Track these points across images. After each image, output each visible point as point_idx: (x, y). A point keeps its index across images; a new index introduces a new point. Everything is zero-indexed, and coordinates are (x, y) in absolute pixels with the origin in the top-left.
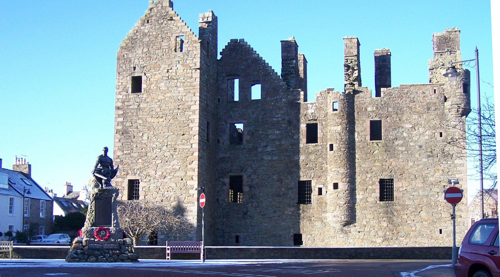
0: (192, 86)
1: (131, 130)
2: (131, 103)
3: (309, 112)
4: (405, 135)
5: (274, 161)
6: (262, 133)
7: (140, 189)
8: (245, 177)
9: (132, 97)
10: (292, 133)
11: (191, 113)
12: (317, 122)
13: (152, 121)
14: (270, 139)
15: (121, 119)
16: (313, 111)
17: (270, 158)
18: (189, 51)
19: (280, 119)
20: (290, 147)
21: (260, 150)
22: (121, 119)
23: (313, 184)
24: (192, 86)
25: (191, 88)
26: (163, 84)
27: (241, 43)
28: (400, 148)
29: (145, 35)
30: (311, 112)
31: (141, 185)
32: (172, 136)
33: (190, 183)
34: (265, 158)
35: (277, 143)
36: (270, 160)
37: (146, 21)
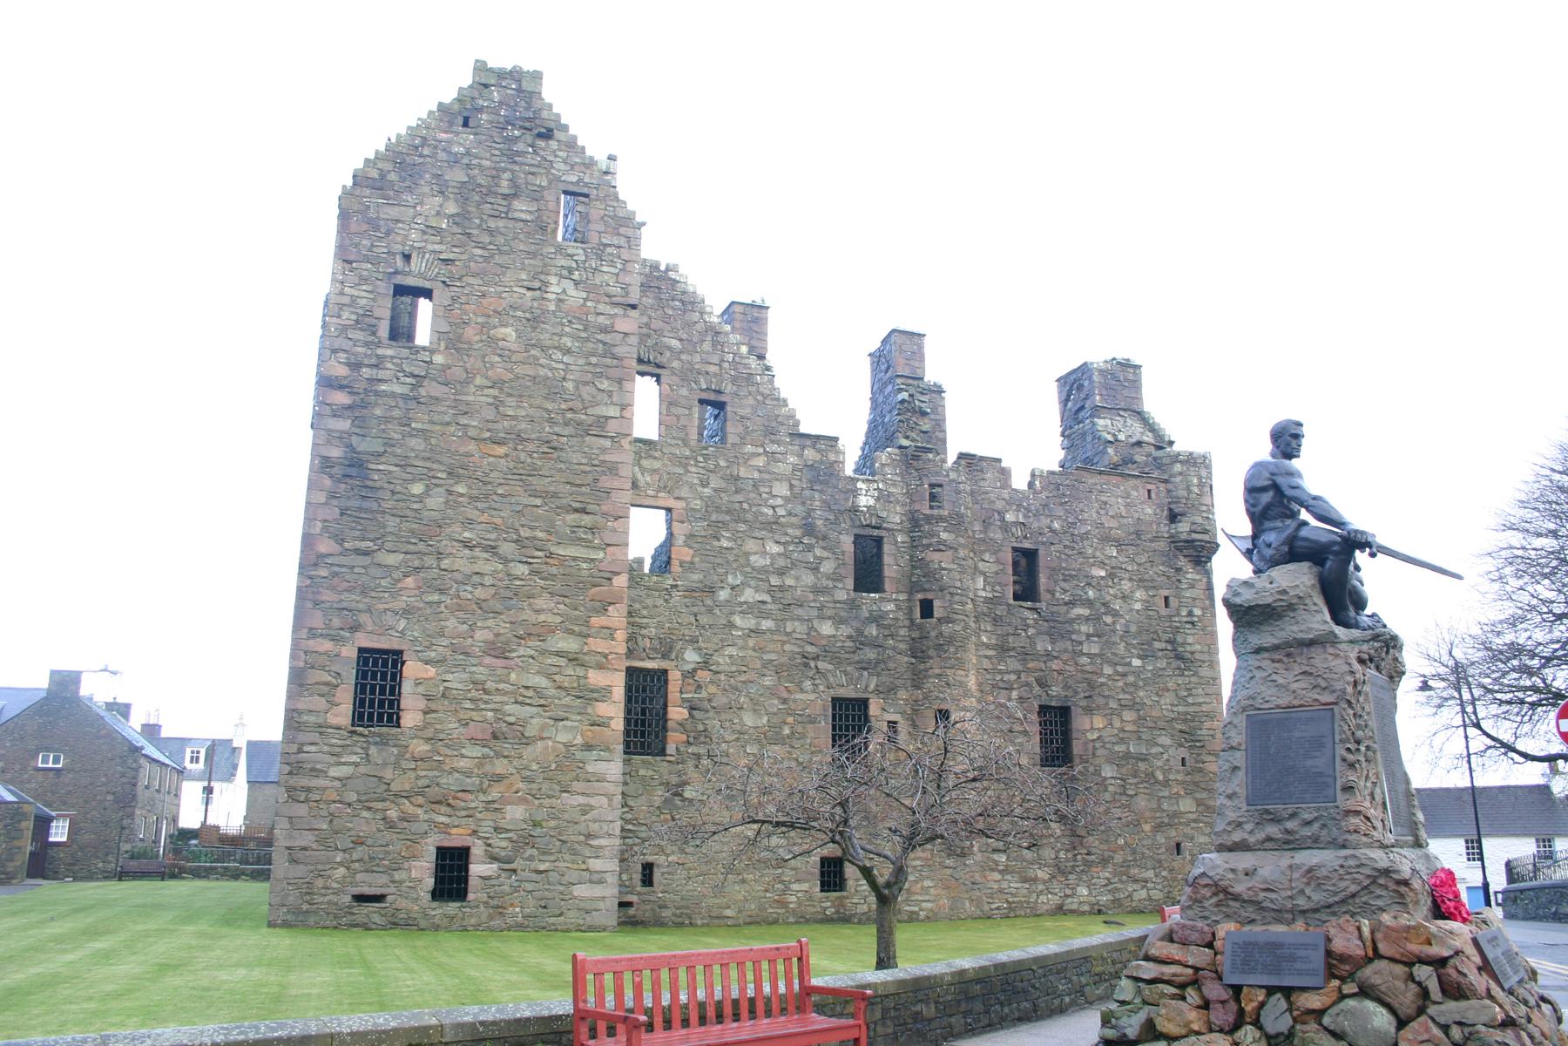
0: (614, 357)
1: (381, 467)
2: (381, 374)
3: (862, 504)
4: (1091, 593)
5: (764, 632)
6: (730, 545)
7: (407, 687)
8: (675, 677)
9: (389, 352)
10: (815, 557)
11: (608, 443)
12: (883, 533)
13: (462, 450)
14: (753, 569)
15: (344, 425)
16: (872, 502)
17: (751, 622)
18: (606, 245)
19: (781, 512)
20: (811, 596)
21: (723, 595)
22: (344, 425)
23: (874, 710)
24: (614, 357)
25: (608, 361)
26: (509, 332)
27: (672, 275)
28: (1084, 628)
29: (455, 160)
30: (865, 504)
31: (412, 669)
32: (535, 509)
33: (595, 678)
34: (737, 620)
35: (774, 581)
36: (751, 630)
37: (460, 121)
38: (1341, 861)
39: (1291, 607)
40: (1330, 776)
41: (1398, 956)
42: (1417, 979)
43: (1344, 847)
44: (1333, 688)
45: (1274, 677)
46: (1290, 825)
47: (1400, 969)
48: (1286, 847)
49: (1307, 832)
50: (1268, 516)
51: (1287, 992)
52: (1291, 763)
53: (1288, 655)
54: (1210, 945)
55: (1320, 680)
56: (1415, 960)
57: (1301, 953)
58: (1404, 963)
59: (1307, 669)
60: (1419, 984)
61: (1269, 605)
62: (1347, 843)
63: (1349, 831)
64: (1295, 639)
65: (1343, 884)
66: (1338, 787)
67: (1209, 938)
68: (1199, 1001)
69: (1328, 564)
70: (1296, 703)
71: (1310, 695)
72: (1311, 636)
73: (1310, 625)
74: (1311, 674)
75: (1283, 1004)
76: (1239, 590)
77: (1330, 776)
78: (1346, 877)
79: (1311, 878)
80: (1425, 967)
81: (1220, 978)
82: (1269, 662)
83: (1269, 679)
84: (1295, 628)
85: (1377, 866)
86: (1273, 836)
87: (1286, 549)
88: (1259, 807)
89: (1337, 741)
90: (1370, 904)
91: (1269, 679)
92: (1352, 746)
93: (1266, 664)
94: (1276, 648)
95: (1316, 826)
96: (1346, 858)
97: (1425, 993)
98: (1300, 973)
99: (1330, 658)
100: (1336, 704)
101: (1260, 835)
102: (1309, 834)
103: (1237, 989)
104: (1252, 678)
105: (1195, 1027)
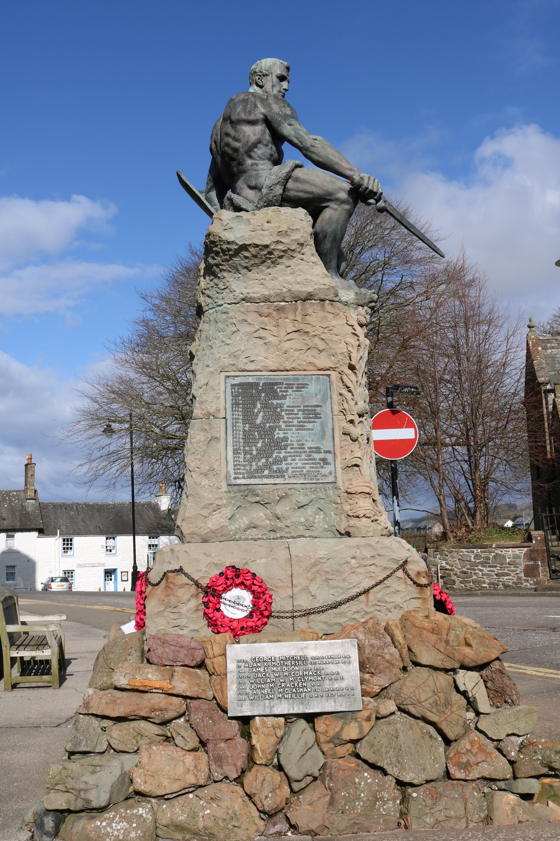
38: (352, 553)
39: (287, 253)
40: (329, 452)
41: (438, 664)
42: (462, 688)
43: (348, 534)
44: (333, 352)
45: (262, 333)
46: (280, 509)
47: (443, 679)
48: (272, 535)
49: (301, 517)
50: (252, 154)
51: (310, 718)
52: (281, 436)
53: (279, 310)
54: (201, 665)
55: (317, 341)
56: (457, 665)
57: (332, 668)
58: (446, 671)
59: (302, 326)
60: (464, 694)
61: (267, 246)
62: (351, 530)
63: (357, 517)
64: (289, 290)
65: (354, 579)
66: (339, 466)
67: (198, 659)
68: (194, 742)
69: (327, 214)
70: (288, 366)
71: (304, 357)
72: (310, 289)
73: (308, 277)
74: (307, 333)
75: (310, 736)
76: (231, 225)
77: (329, 452)
78: (359, 570)
79: (317, 572)
80: (470, 673)
81: (225, 711)
82: (255, 315)
83: (256, 335)
84: (290, 278)
85: (394, 556)
86: (259, 523)
87: (279, 190)
88: (243, 488)
89: (336, 412)
90: (386, 602)
91: (256, 335)
92: (357, 419)
93: (252, 317)
94: (267, 300)
95: (310, 510)
96: (358, 547)
97: (471, 704)
98: (330, 694)
99: (330, 316)
100: (334, 369)
101: (243, 521)
102: (303, 520)
103: (245, 721)
104: (234, 332)
105: (191, 779)
